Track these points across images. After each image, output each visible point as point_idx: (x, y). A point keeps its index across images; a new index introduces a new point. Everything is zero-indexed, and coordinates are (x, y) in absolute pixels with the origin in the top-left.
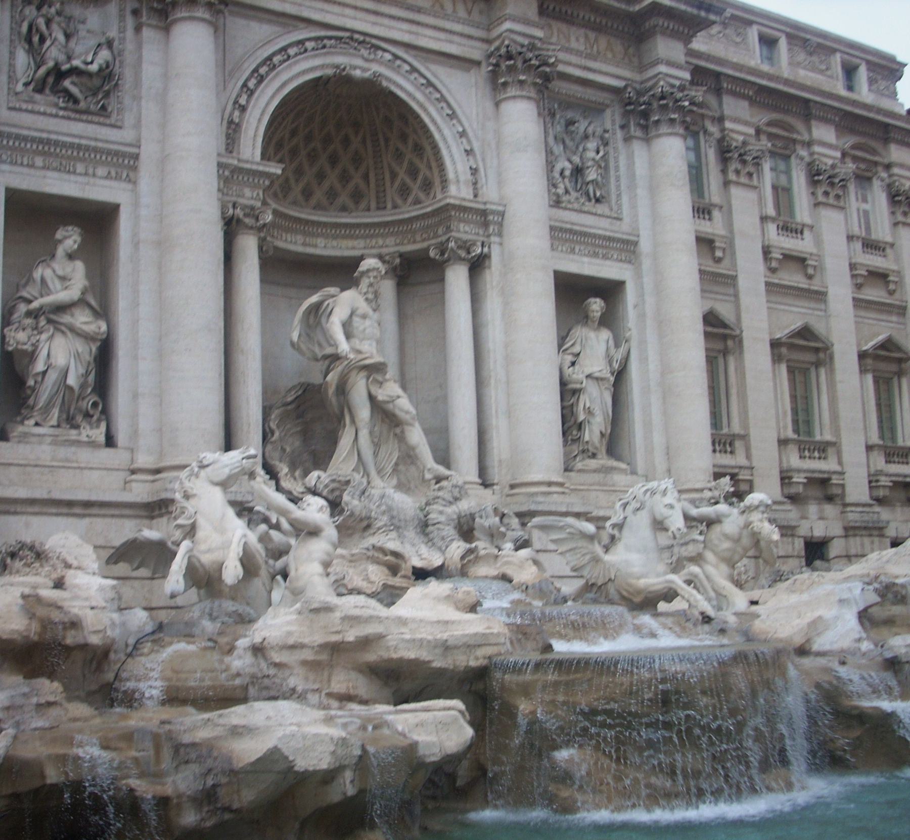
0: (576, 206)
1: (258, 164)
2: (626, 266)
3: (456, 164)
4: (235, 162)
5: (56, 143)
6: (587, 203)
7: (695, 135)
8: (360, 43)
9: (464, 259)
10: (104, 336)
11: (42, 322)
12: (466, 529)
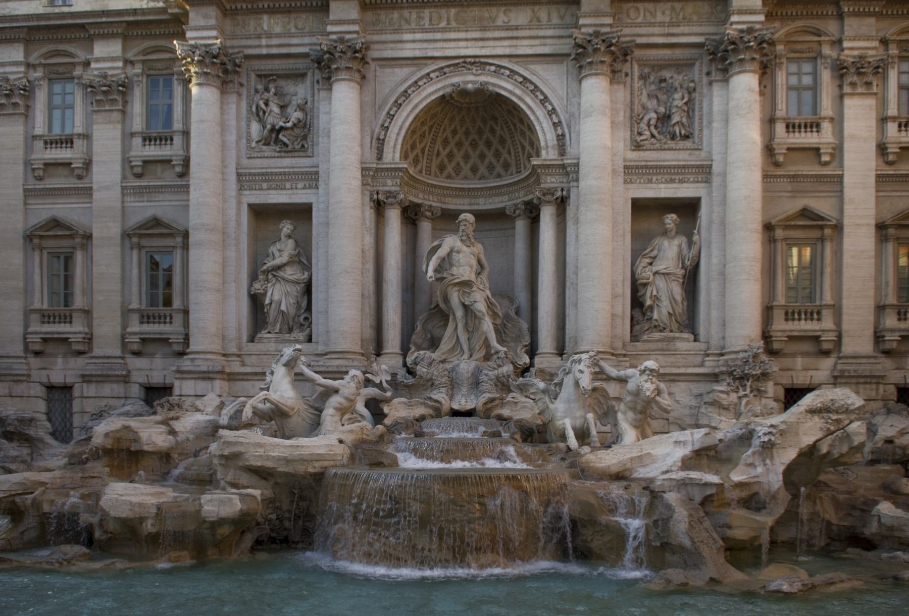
0: (658, 145)
1: (391, 164)
2: (702, 185)
3: (546, 134)
4: (375, 166)
5: (272, 174)
9: (549, 202)
12: (503, 385)
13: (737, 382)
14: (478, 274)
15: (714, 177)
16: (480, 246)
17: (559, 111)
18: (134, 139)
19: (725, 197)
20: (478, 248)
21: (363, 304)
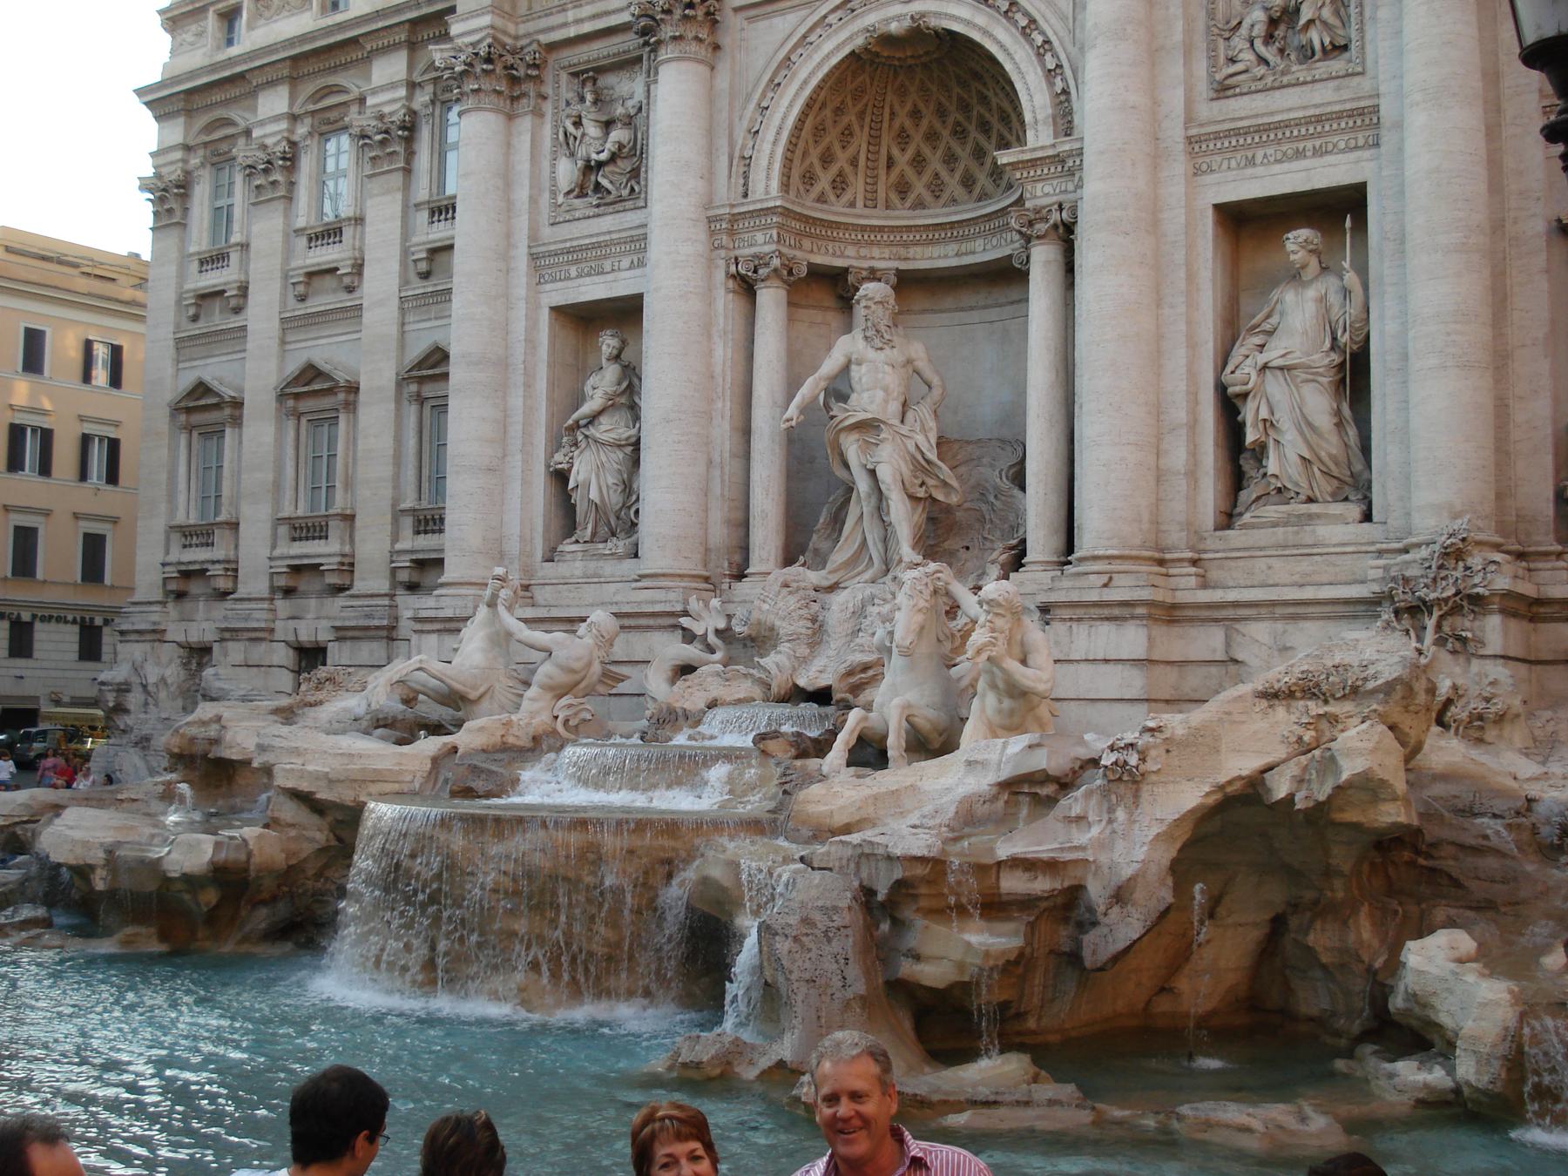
2: (1367, 154)
3: (1034, 97)
4: (727, 210)
5: (581, 249)
6: (1294, 68)
13: (1406, 622)
17: (1056, 43)
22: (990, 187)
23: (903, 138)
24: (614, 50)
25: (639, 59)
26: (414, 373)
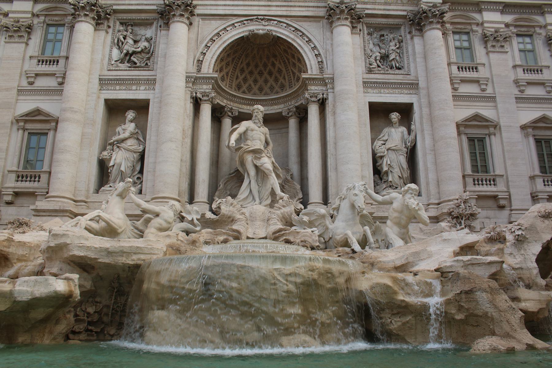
2: (413, 96)
4: (195, 75)
5: (123, 80)
7: (468, 33)
8: (262, 20)
9: (314, 102)
10: (141, 150)
11: (115, 147)
13: (455, 220)
14: (265, 148)
15: (421, 91)
16: (267, 129)
18: (32, 61)
19: (430, 103)
20: (265, 130)
21: (181, 166)
22: (269, 91)
23: (242, 71)
24: (143, 18)
25: (151, 24)
26: (24, 118)
